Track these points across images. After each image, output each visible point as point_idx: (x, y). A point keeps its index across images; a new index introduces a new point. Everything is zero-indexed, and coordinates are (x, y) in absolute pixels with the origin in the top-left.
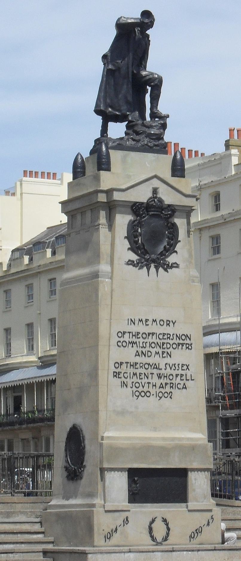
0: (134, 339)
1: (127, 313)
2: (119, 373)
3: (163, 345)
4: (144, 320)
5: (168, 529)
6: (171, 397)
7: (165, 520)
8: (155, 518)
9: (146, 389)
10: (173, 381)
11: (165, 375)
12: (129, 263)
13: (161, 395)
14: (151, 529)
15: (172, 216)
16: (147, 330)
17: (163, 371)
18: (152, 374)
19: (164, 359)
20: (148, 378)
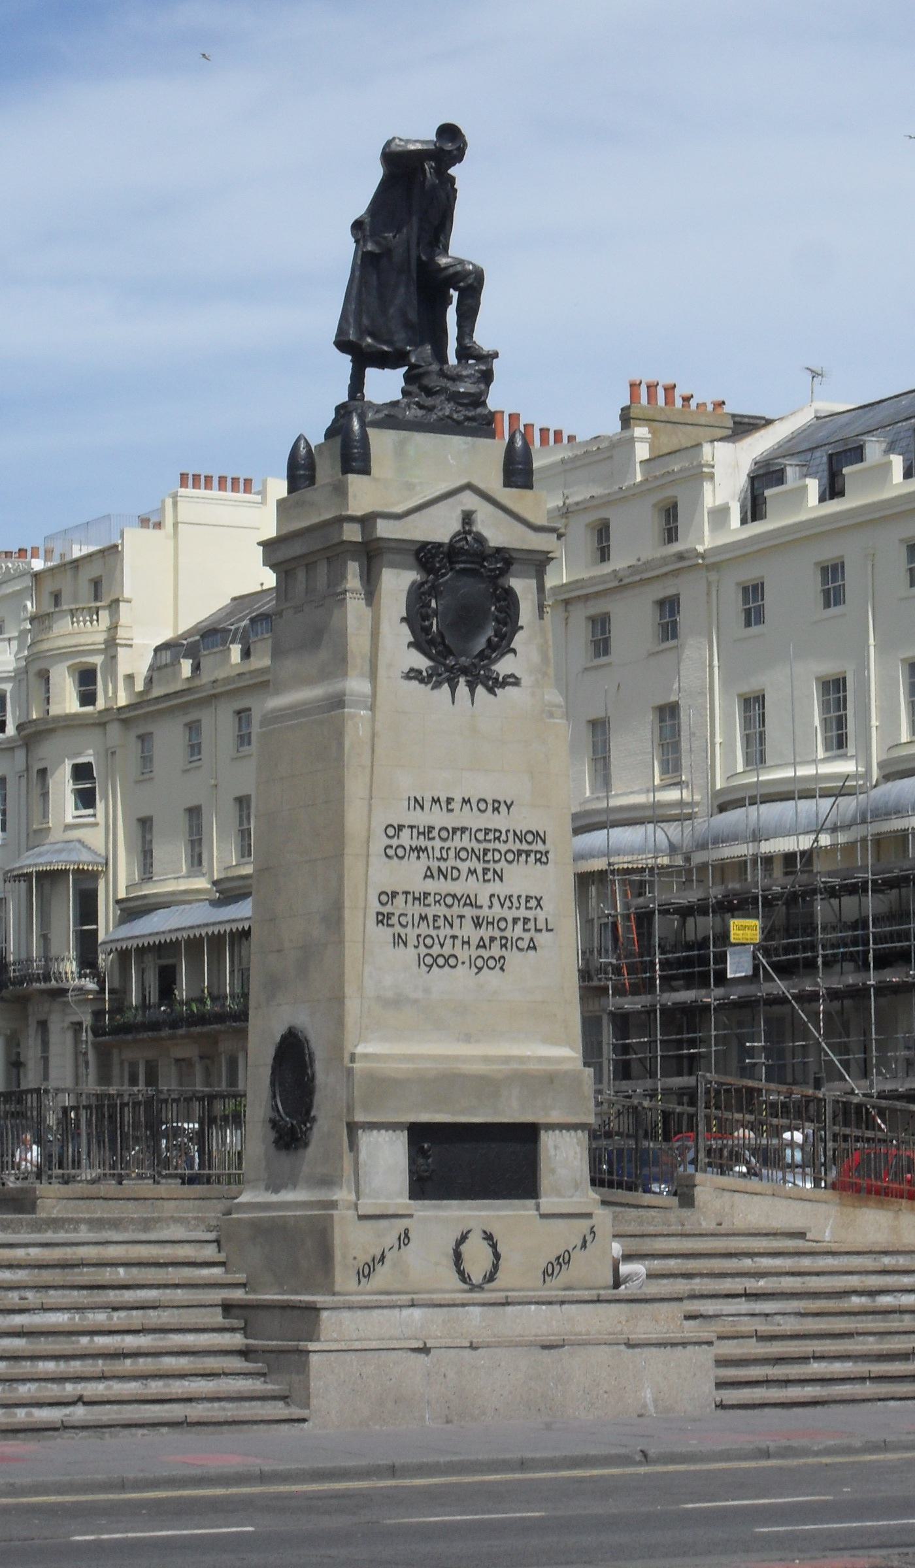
0: (422, 842)
1: (407, 784)
2: (390, 915)
3: (485, 854)
4: (443, 800)
5: (497, 1256)
6: (502, 969)
7: (488, 1237)
8: (469, 1232)
9: (447, 951)
10: (508, 934)
11: (490, 920)
12: (412, 675)
13: (480, 963)
14: (458, 1257)
15: (504, 572)
16: (450, 821)
17: (485, 912)
18: (461, 917)
19: (487, 884)
20: (451, 926)
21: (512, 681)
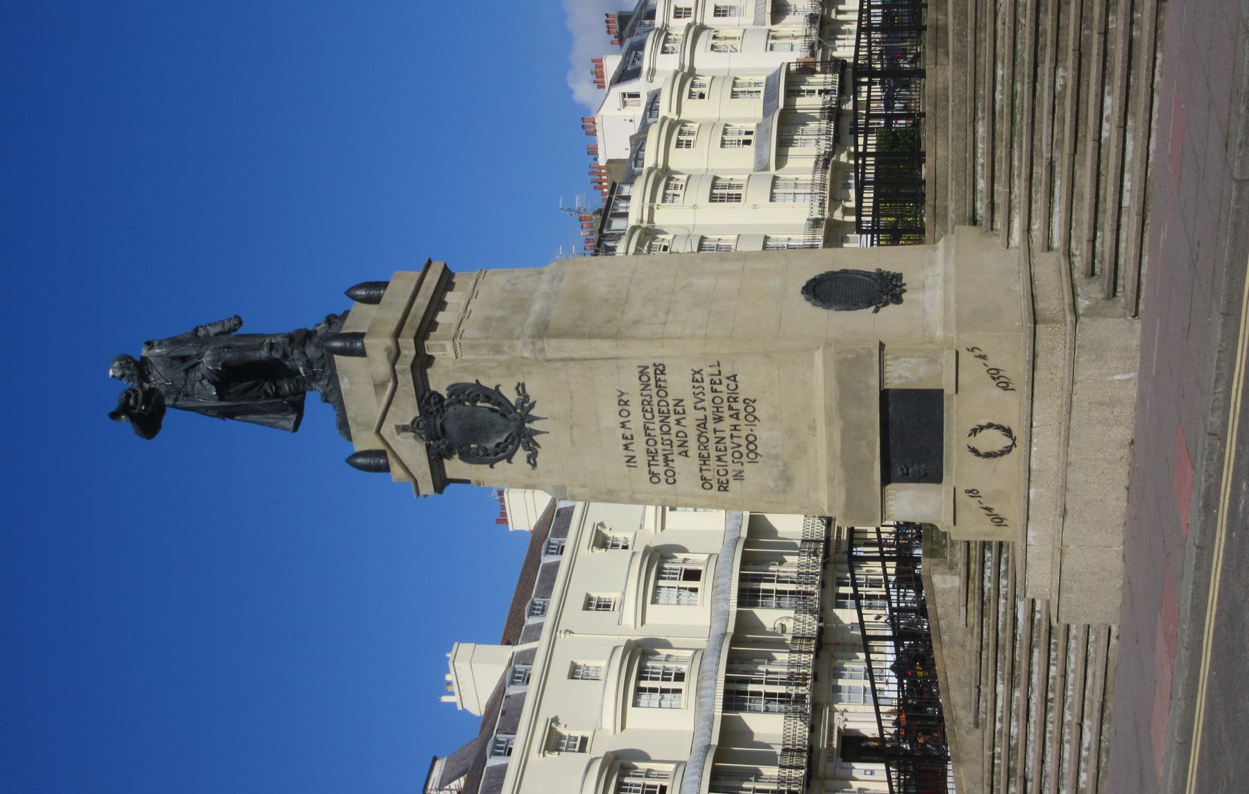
0: (660, 458)
4: (625, 442)
5: (990, 426)
7: (974, 431)
9: (743, 442)
10: (725, 396)
14: (988, 455)
17: (709, 413)
18: (715, 431)
20: (723, 438)
21: (521, 388)
